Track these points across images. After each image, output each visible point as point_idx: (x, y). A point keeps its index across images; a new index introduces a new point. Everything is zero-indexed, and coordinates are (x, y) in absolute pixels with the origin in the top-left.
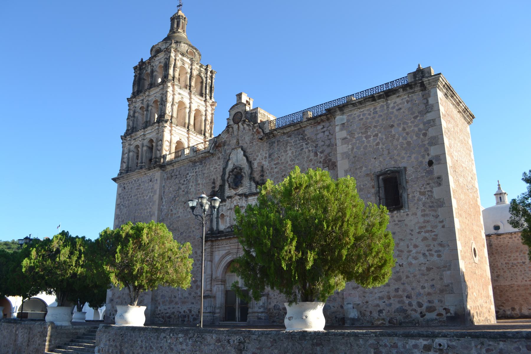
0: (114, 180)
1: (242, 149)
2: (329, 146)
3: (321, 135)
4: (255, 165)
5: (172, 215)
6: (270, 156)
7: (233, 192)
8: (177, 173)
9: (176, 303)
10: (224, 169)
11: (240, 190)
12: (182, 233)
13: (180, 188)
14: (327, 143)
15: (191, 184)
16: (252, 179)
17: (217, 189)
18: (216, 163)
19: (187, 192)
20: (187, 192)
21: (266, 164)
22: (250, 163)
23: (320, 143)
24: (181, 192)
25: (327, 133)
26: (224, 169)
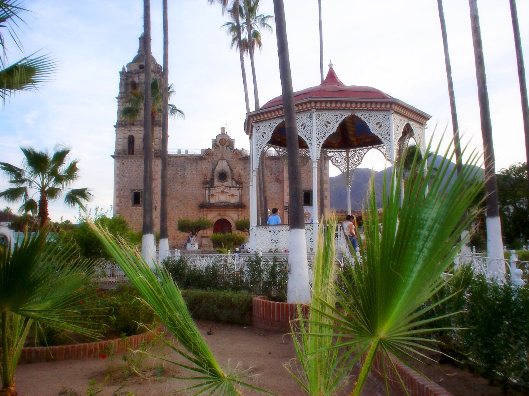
0: (113, 156)
1: (227, 162)
2: (278, 172)
3: (274, 166)
4: (235, 171)
5: (171, 189)
6: (244, 169)
7: (220, 184)
8: (174, 164)
9: (179, 240)
10: (213, 170)
11: (225, 184)
12: (181, 201)
13: (177, 173)
14: (278, 170)
15: (187, 172)
16: (233, 179)
17: (208, 180)
18: (207, 164)
19: (184, 177)
20: (184, 177)
21: (242, 172)
22: (231, 170)
23: (274, 170)
24: (178, 176)
25: (277, 165)
26: (213, 170)
